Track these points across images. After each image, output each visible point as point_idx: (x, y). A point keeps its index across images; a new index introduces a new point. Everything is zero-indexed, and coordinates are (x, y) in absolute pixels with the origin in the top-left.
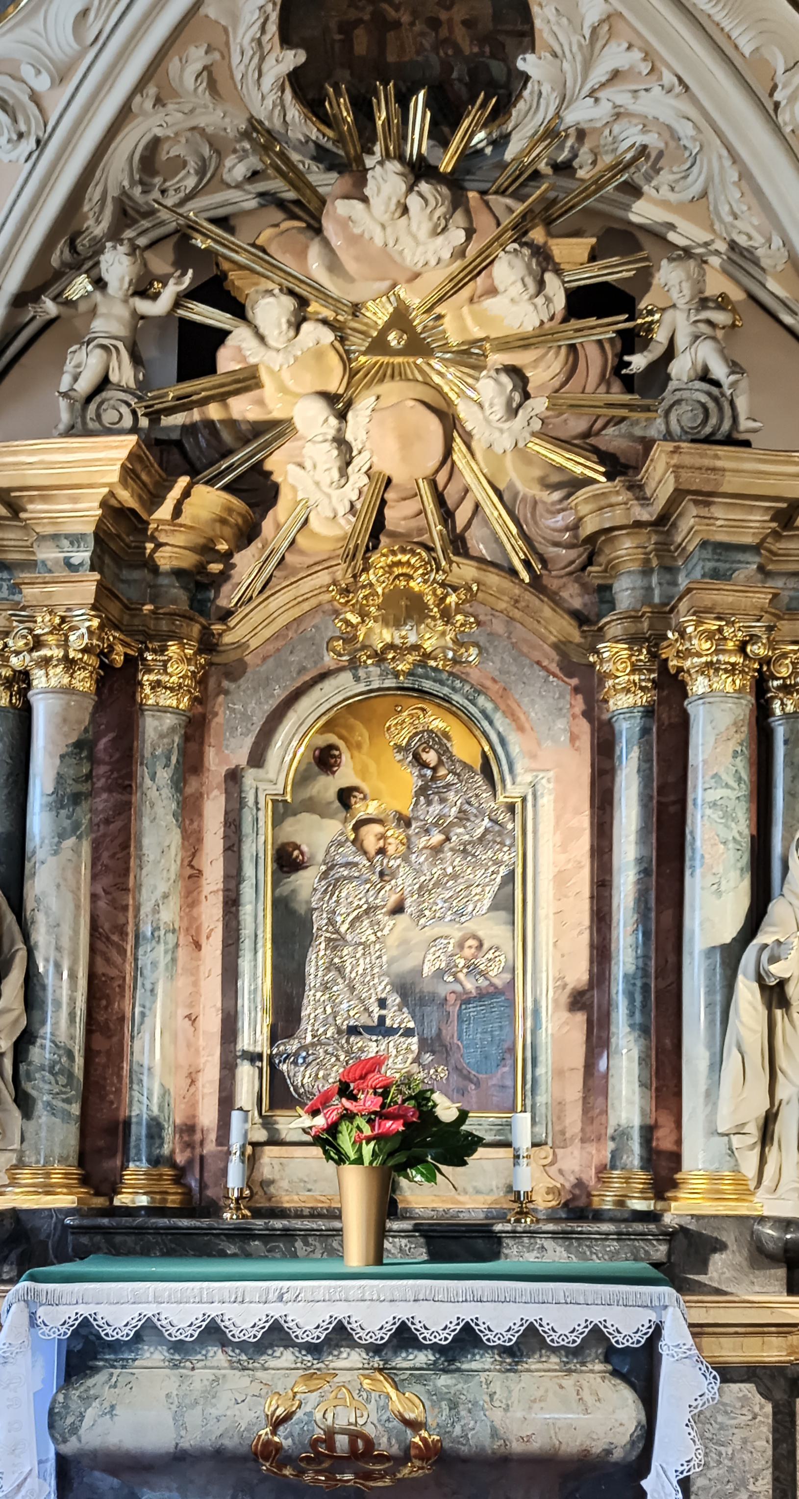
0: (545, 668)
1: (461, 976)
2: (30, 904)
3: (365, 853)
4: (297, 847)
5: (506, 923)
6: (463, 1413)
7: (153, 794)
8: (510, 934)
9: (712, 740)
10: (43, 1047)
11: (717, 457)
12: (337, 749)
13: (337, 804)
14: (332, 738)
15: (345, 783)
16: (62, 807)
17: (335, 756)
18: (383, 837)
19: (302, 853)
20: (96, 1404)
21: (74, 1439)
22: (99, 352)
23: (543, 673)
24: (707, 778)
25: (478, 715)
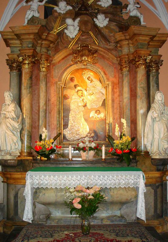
0: (110, 64)
1: (96, 118)
2: (22, 106)
3: (79, 96)
4: (67, 95)
5: (104, 108)
6: (106, 193)
7: (42, 86)
8: (105, 110)
9: (141, 76)
10: (25, 131)
11: (141, 29)
12: (74, 78)
13: (74, 87)
14: (73, 76)
15: (75, 84)
16: (28, 89)
17: (73, 79)
18: (82, 93)
19: (68, 96)
20: (42, 193)
21: (38, 199)
22: (33, 11)
23: (109, 65)
24: (140, 83)
25: (98, 72)
